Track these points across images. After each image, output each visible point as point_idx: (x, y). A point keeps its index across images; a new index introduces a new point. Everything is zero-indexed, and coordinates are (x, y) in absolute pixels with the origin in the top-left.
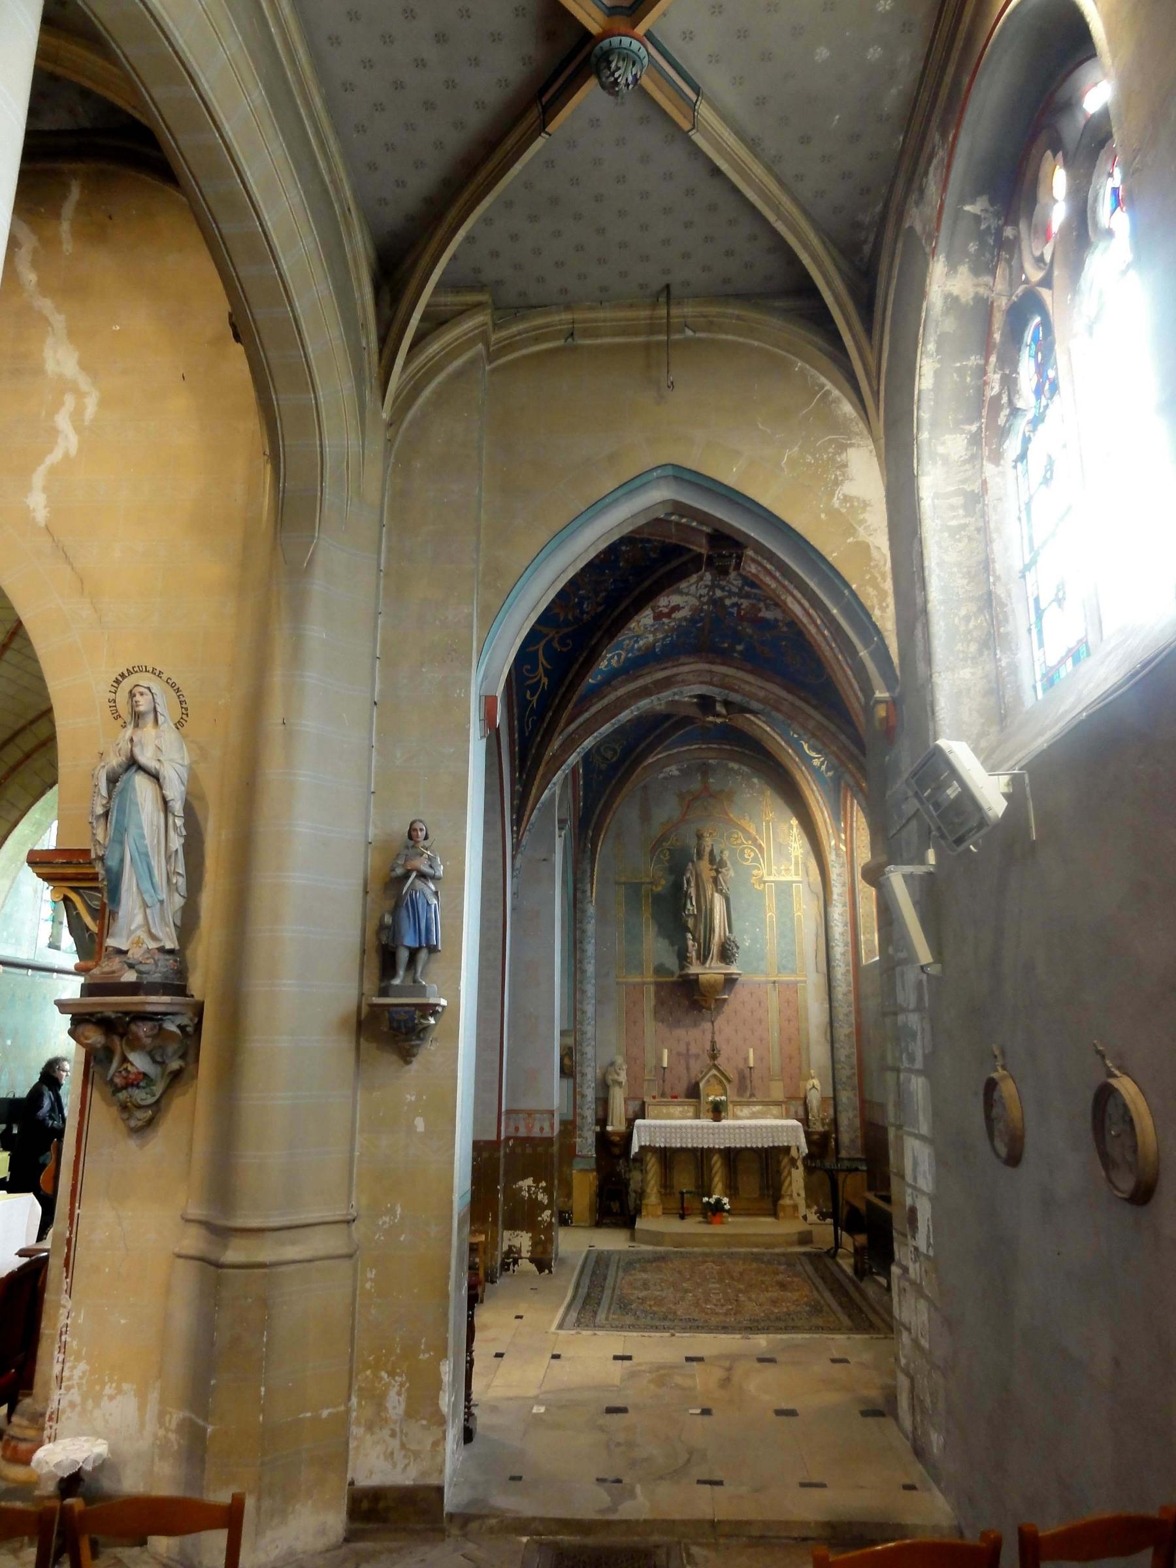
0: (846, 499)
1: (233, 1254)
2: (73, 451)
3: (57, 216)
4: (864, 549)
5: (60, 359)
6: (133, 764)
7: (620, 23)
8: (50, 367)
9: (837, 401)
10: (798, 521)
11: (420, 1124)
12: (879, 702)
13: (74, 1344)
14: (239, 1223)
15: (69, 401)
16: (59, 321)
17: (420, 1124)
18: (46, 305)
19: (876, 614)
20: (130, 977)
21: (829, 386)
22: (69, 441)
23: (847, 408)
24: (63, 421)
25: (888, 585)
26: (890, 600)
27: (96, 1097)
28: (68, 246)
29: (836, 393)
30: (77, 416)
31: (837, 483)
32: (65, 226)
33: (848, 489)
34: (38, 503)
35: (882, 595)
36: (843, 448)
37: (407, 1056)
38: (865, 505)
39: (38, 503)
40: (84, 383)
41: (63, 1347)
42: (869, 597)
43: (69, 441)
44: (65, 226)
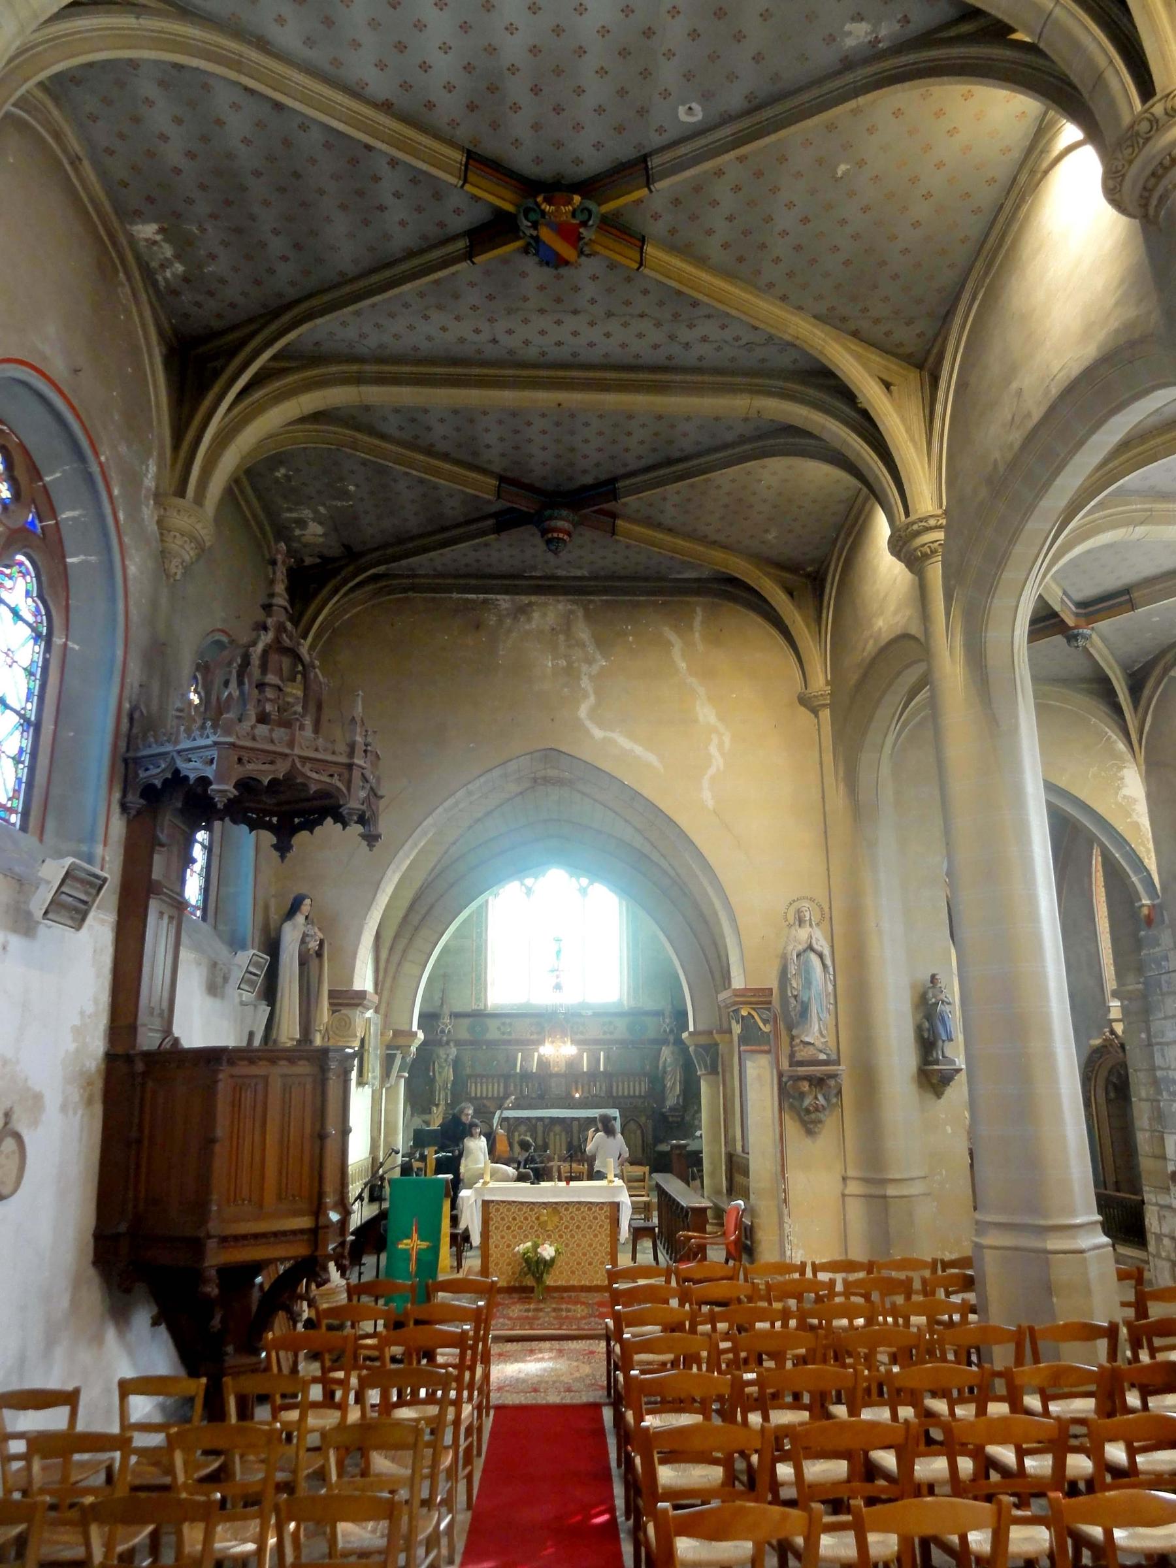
0: (1125, 797)
1: (891, 1191)
2: (722, 767)
3: (691, 628)
4: (1136, 826)
5: (706, 714)
6: (811, 948)
7: (1082, 621)
8: (701, 718)
9: (1115, 742)
10: (1100, 809)
11: (949, 1130)
12: (1143, 905)
13: (795, 1241)
14: (891, 1177)
15: (715, 739)
16: (701, 691)
17: (949, 1130)
18: (693, 681)
19: (1146, 862)
20: (823, 1057)
21: (1110, 733)
22: (718, 762)
23: (1121, 746)
24: (713, 749)
25: (1151, 846)
26: (1153, 854)
27: (787, 1117)
28: (701, 647)
29: (1114, 737)
30: (720, 746)
31: (1119, 788)
32: (697, 635)
33: (1125, 791)
34: (707, 796)
35: (1148, 851)
36: (1121, 768)
37: (939, 1094)
38: (1135, 801)
39: (707, 796)
40: (721, 728)
41: (790, 1242)
42: (1141, 851)
43: (718, 762)
44: (697, 635)
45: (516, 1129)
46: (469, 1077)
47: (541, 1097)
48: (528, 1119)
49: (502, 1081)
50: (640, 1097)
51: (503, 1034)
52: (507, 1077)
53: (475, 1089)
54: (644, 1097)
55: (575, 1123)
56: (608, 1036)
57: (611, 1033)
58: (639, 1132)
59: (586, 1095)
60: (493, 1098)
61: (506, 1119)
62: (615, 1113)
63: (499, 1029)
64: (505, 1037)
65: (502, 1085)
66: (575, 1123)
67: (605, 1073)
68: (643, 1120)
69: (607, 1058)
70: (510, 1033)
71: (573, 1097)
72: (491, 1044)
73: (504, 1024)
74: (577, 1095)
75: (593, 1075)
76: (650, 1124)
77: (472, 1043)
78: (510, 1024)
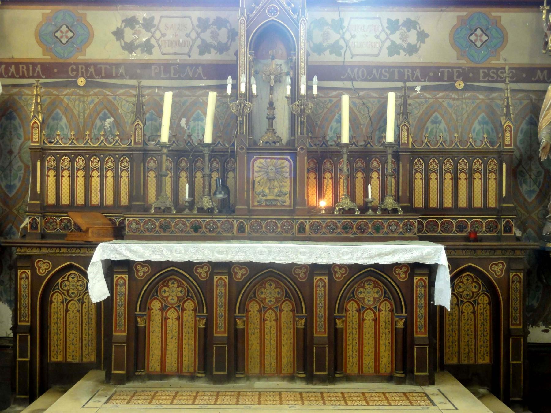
45: (153, 292)
46: (41, 153)
47: (226, 207)
48: (189, 266)
49: (125, 162)
50: (485, 210)
51: (130, 47)
52: (140, 155)
53: (57, 186)
54: (498, 212)
55: (320, 280)
56: (401, 58)
57: (412, 50)
58: (484, 300)
59: (346, 203)
60: (101, 208)
61: (126, 265)
62: (434, 253)
63: (118, 34)
64: (135, 56)
65: (125, 181)
66: (320, 280)
67: (398, 152)
68: (496, 271)
69: (403, 112)
70: (147, 47)
71: (314, 211)
72: (98, 72)
73: (131, 22)
74: (324, 203)
75: (365, 154)
76: (517, 276)
77: (47, 69)
78: (148, 24)
